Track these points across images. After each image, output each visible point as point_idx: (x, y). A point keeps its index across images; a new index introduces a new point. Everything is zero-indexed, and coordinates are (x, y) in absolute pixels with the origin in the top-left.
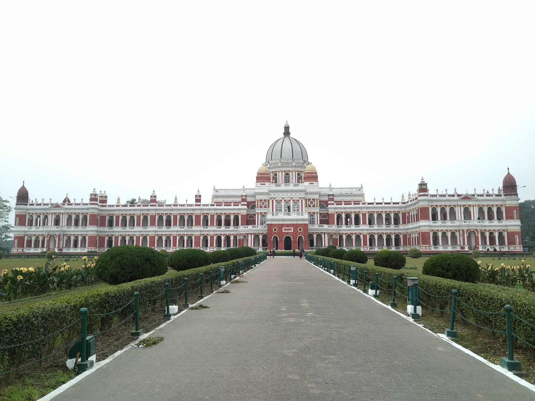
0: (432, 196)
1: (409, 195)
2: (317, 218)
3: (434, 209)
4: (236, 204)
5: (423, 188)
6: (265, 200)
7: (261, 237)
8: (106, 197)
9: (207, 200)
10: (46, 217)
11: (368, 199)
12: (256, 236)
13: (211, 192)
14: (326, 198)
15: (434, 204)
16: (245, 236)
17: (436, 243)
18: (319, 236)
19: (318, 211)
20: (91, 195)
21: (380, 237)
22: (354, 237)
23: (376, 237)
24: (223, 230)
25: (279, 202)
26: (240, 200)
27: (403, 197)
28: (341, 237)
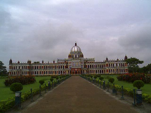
0: (109, 61)
1: (105, 60)
2: (83, 66)
3: (109, 64)
4: (63, 63)
5: (107, 59)
6: (71, 62)
7: (70, 71)
8: (31, 62)
9: (56, 62)
10: (17, 67)
11: (95, 61)
12: (69, 71)
13: (57, 60)
14: (85, 61)
15: (109, 63)
16: (65, 71)
17: (110, 72)
18: (84, 71)
19: (83, 64)
20: (28, 61)
21: (98, 71)
22: (92, 71)
23: (97, 71)
24: (60, 70)
25: (74, 63)
26: (64, 62)
27: (104, 61)
28: (89, 71)
